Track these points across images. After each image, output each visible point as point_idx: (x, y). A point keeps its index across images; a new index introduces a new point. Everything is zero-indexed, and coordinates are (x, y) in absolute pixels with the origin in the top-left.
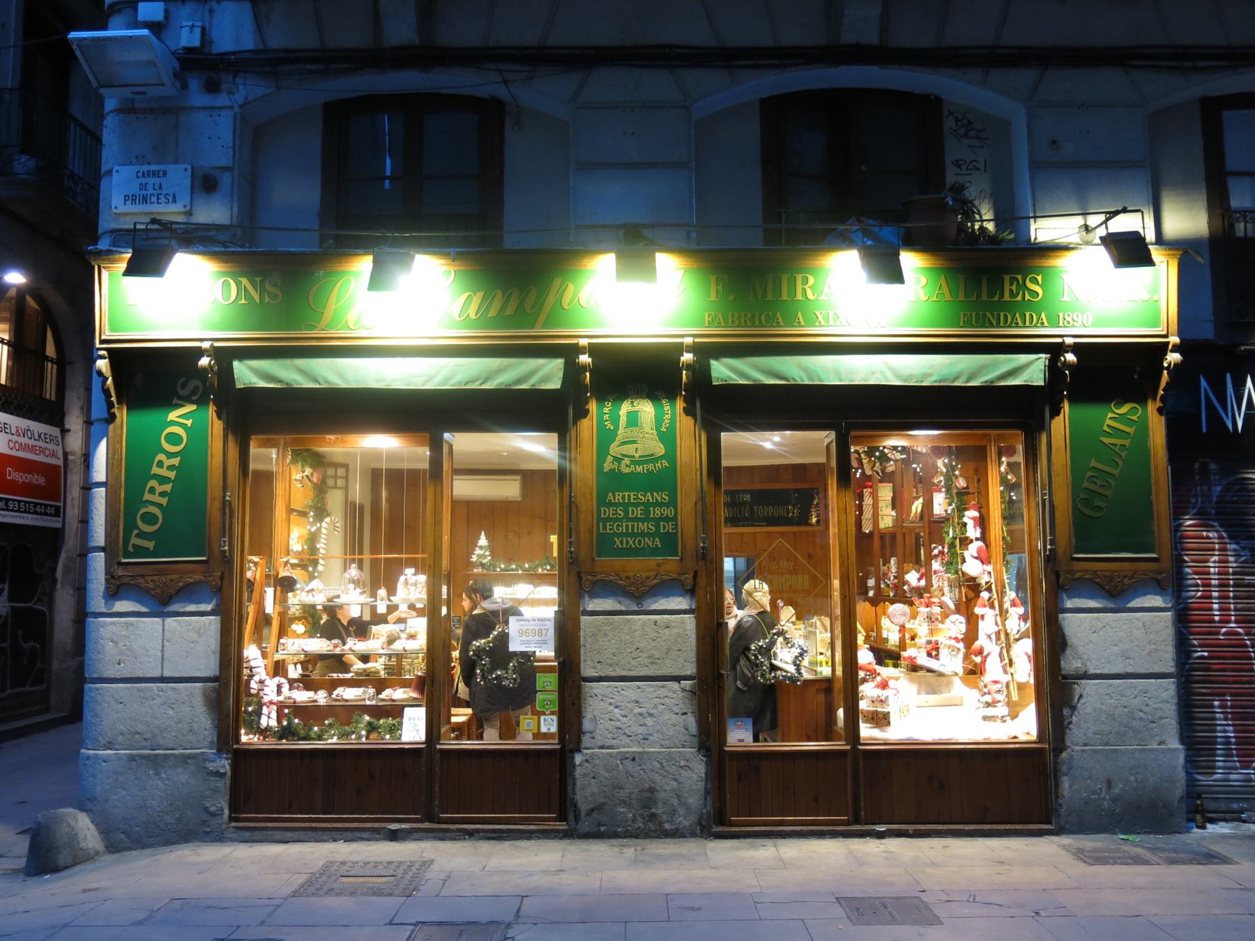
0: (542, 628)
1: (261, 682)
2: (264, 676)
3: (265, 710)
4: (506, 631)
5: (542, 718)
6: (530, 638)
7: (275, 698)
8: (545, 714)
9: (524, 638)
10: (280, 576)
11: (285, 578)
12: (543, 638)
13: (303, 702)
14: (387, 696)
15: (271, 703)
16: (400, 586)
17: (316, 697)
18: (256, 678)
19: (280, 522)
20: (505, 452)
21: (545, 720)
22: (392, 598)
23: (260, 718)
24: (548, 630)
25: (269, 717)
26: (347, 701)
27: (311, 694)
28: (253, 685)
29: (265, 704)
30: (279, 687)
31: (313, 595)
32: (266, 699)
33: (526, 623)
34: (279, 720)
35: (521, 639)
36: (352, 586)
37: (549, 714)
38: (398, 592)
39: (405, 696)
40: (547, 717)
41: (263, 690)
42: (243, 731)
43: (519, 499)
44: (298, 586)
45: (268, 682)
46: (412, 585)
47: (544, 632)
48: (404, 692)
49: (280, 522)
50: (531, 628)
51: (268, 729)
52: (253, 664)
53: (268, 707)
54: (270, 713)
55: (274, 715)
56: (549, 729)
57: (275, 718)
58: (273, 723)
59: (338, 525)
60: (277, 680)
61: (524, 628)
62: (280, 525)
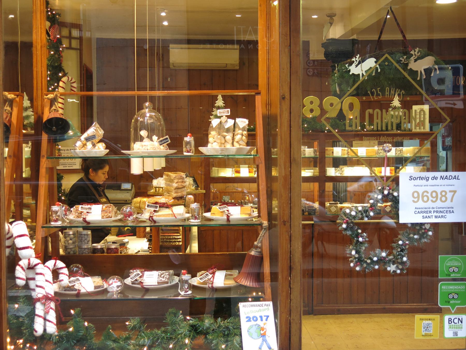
0: (447, 189)
1: (31, 268)
2: (35, 261)
3: (39, 309)
4: (395, 194)
5: (446, 318)
6: (429, 204)
7: (52, 289)
8: (448, 311)
9: (421, 204)
10: (45, 119)
11: (50, 121)
12: (448, 204)
13: (89, 294)
14: (205, 283)
15: (47, 298)
16: (213, 136)
17: (106, 286)
18: (24, 263)
19: (39, 47)
20: (240, 10)
21: (450, 320)
22: (201, 149)
23: (32, 321)
24: (455, 192)
25: (45, 319)
26: (147, 290)
27: (98, 280)
28: (19, 273)
29: (38, 300)
30: (56, 273)
31: (94, 145)
32: (38, 293)
33: (424, 182)
34: (60, 323)
35: (418, 205)
36: (143, 133)
37: (456, 313)
38: (211, 139)
39: (231, 283)
40: (453, 317)
41: (34, 279)
42: (8, 340)
43: (237, 68)
44: (71, 133)
45: (40, 268)
46: (228, 130)
47: (449, 195)
48: (226, 276)
49: (39, 47)
50: (430, 189)
51: (45, 337)
52: (20, 243)
53: (44, 304)
54: (47, 313)
55: (52, 316)
56: (456, 334)
57: (54, 321)
58: (52, 329)
59: (75, 85)
60: (51, 263)
61: (421, 190)
62: (39, 53)
